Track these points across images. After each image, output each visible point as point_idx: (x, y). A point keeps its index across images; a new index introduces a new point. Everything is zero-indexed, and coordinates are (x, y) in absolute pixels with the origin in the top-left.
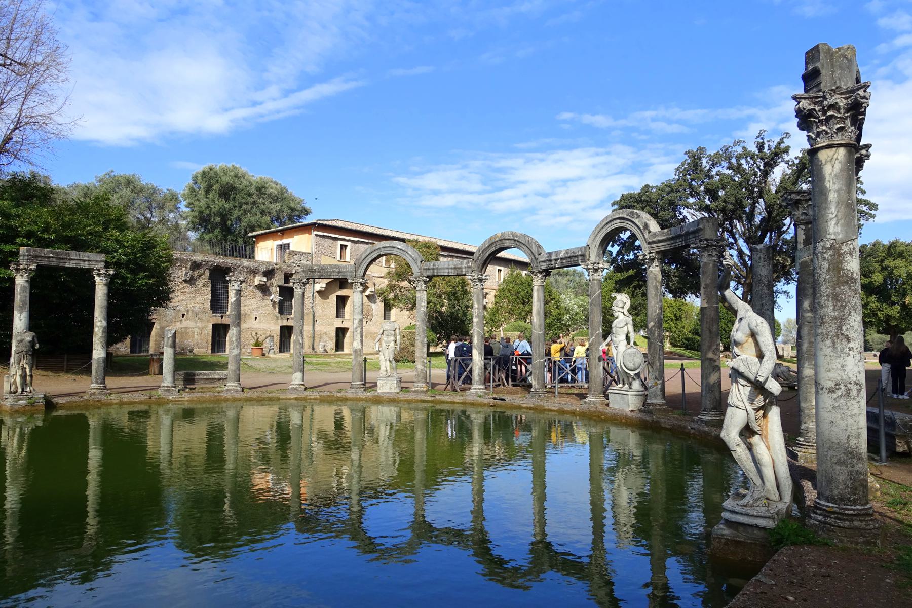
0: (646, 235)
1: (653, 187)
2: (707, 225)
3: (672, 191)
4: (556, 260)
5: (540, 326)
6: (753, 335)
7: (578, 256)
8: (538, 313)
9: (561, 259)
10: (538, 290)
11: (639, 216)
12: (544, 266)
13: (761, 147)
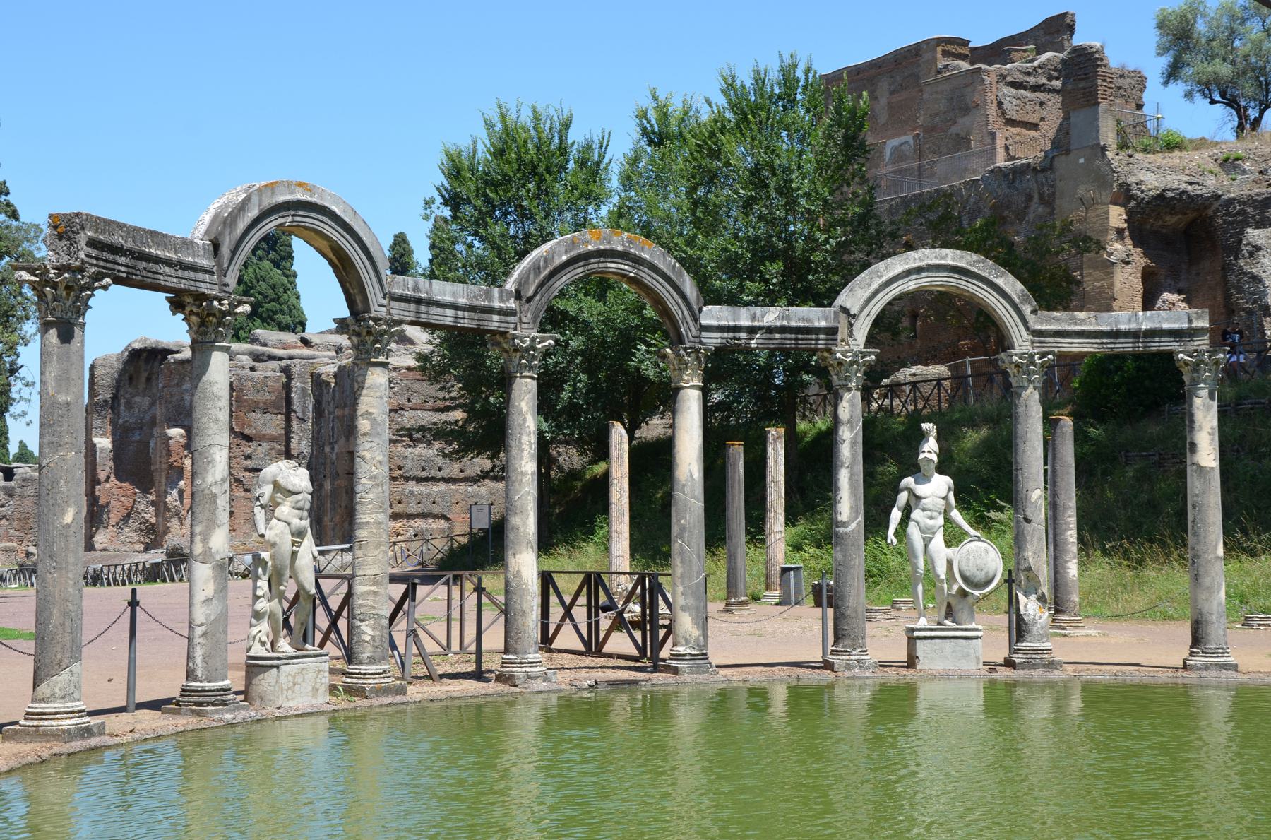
4: (752, 330)
7: (817, 331)
9: (770, 330)
12: (713, 340)
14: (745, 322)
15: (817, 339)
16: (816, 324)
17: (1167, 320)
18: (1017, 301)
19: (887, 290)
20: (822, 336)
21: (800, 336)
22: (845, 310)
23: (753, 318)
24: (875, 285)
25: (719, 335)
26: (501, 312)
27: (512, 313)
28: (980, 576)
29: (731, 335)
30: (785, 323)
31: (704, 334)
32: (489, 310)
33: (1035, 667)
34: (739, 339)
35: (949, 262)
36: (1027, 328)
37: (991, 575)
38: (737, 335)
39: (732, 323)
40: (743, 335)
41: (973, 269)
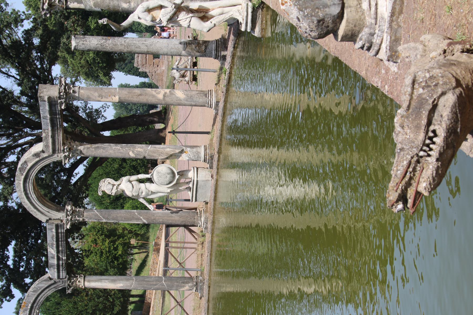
2: (45, 93)
4: (58, 259)
6: (149, 10)
7: (57, 233)
8: (113, 281)
9: (58, 252)
10: (89, 281)
11: (26, 162)
12: (63, 274)
14: (55, 262)
15: (61, 233)
16: (55, 234)
17: (44, 108)
18: (38, 159)
19: (37, 206)
20: (60, 231)
21: (60, 240)
22: (47, 221)
23: (53, 258)
24: (35, 210)
25: (61, 272)
28: (169, 177)
29: (61, 267)
30: (55, 246)
31: (61, 277)
34: (63, 264)
35: (22, 182)
36: (52, 155)
37: (169, 171)
38: (61, 265)
39: (56, 267)
40: (61, 262)
41: (24, 174)
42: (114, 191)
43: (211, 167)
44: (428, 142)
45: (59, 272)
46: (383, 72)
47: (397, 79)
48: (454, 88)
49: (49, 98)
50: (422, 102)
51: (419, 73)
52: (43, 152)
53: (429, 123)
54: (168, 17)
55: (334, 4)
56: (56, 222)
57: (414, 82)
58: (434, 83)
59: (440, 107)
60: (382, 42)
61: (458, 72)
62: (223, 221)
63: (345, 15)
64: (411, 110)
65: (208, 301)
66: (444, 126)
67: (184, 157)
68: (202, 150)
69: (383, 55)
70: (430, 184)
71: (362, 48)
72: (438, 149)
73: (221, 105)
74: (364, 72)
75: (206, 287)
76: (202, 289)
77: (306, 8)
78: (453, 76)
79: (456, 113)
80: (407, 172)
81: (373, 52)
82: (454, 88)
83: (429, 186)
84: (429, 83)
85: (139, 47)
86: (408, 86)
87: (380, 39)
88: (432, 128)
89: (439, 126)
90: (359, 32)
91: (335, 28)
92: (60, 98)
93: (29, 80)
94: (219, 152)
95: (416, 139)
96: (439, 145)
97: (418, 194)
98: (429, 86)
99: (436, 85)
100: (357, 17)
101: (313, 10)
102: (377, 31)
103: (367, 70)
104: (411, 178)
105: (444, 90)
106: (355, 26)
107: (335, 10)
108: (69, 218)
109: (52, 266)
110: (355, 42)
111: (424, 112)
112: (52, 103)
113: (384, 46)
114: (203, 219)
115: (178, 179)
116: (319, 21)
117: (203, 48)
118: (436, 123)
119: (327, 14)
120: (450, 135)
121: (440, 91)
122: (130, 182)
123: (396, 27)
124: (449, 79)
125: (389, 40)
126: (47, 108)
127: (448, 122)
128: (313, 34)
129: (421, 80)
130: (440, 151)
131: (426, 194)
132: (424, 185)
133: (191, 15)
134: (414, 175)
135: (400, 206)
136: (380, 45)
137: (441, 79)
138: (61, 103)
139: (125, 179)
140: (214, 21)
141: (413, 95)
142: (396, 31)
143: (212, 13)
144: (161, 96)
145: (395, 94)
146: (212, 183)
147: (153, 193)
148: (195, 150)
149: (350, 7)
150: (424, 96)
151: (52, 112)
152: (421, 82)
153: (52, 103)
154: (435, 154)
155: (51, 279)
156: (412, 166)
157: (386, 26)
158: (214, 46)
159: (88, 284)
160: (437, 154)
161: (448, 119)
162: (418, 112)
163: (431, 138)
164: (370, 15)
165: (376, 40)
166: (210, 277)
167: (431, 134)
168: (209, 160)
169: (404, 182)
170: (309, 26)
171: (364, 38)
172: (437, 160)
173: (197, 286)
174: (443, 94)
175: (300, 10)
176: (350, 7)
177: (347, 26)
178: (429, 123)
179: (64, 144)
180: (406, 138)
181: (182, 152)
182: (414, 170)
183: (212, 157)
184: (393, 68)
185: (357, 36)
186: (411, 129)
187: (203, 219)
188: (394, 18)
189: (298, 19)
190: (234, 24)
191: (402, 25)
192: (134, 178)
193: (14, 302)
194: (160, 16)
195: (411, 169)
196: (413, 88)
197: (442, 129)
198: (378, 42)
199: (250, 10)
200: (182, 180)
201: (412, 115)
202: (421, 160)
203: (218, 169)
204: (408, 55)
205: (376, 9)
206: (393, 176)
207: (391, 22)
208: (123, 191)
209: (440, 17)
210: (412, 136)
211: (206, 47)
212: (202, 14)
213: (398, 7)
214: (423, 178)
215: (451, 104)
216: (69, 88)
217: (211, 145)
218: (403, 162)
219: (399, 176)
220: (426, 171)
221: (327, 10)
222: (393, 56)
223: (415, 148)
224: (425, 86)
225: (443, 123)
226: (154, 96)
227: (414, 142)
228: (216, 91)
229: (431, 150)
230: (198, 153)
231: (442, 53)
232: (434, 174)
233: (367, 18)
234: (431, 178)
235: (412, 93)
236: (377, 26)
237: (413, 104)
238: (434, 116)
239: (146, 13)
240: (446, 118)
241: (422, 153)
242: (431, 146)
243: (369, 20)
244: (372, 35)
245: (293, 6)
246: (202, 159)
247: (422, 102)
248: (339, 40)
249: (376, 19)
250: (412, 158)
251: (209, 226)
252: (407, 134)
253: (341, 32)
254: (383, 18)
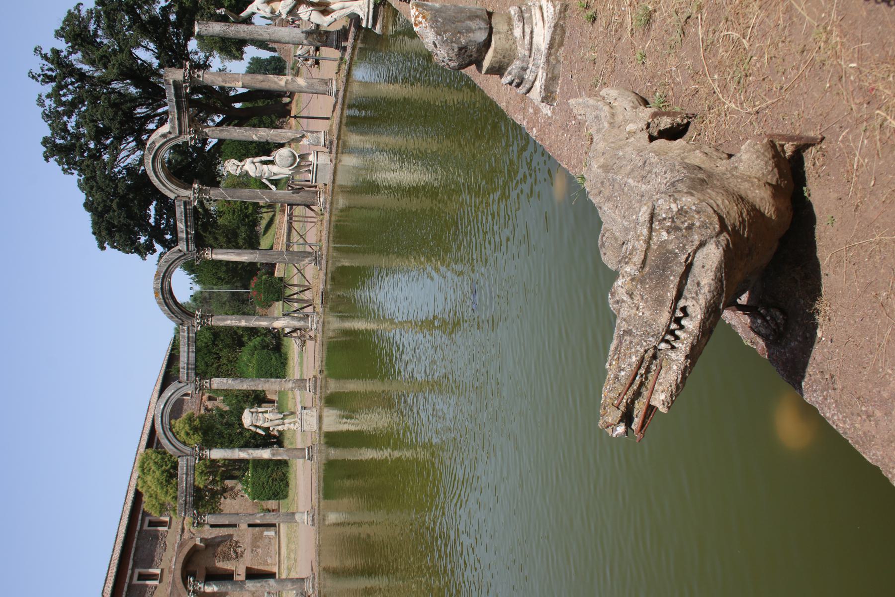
0: (172, 136)
1: (87, 199)
3: (93, 178)
4: (187, 233)
5: (252, 253)
8: (239, 254)
9: (187, 226)
10: (216, 254)
11: (153, 142)
12: (192, 247)
13: (51, 79)
14: (184, 236)
23: (182, 232)
26: (188, 333)
27: (188, 328)
28: (290, 160)
32: (188, 337)
33: (331, 148)
42: (238, 172)
43: (330, 152)
44: (673, 326)
45: (188, 245)
46: (531, 111)
47: (550, 124)
48: (718, 235)
49: (174, 82)
50: (666, 258)
51: (660, 202)
52: (170, 133)
53: (679, 296)
54: (288, 9)
55: (480, 29)
56: (184, 199)
57: (652, 216)
58: (686, 224)
59: (696, 269)
60: (535, 79)
61: (720, 202)
62: (342, 202)
63: (493, 43)
64: (647, 269)
65: (326, 274)
66: (702, 302)
67: (305, 142)
68: (322, 135)
69: (536, 94)
70: (671, 396)
71: (511, 83)
72: (690, 340)
73: (341, 94)
74: (504, 104)
75: (324, 262)
76: (320, 263)
77: (445, 32)
78: (715, 211)
79: (721, 281)
80: (636, 375)
81: (522, 90)
82: (718, 235)
83: (669, 399)
84: (678, 222)
85: (261, 35)
86: (642, 225)
87: (534, 75)
88: (682, 303)
89: (694, 302)
90: (508, 65)
91: (480, 59)
92: (184, 82)
93: (166, 54)
94: (339, 138)
95: (655, 320)
96: (690, 333)
97: (650, 409)
98: (677, 229)
99: (690, 228)
100: (507, 46)
101: (454, 35)
102: (530, 66)
103: (508, 102)
104: (642, 384)
105: (703, 238)
106: (504, 57)
107: (481, 36)
108: (196, 196)
109: (182, 239)
110: (501, 75)
111: (672, 278)
112: (177, 86)
113: (538, 84)
114: (322, 200)
115: (300, 161)
116: (460, 49)
117: (325, 38)
118: (689, 296)
119: (470, 41)
120: (710, 316)
121: (696, 239)
122: (254, 163)
123: (554, 62)
124: (709, 217)
125: (544, 78)
126: (173, 91)
127: (709, 296)
128: (452, 64)
129: (664, 216)
130: (692, 343)
131: (663, 409)
132: (662, 397)
133: (311, 8)
134: (646, 378)
135: (621, 429)
136: (534, 82)
137: (697, 216)
138: (186, 87)
139: (248, 160)
140: (334, 15)
141: (651, 242)
142: (554, 67)
143: (333, 7)
144: (282, 83)
145: (547, 143)
146: (332, 166)
147: (275, 174)
148: (315, 135)
149: (499, 33)
150: (671, 247)
151: (178, 95)
152: (665, 219)
153: (177, 86)
154: (683, 347)
155: (180, 251)
156: (645, 365)
157: (541, 61)
158: (335, 37)
159: (214, 257)
160: (688, 349)
161: (709, 292)
162: (661, 275)
163: (678, 321)
164: (523, 45)
165: (529, 76)
166: (328, 252)
167: (679, 314)
168: (329, 145)
169: (630, 393)
170: (448, 54)
171: (514, 72)
172: (687, 357)
173: (317, 260)
174: (702, 244)
175: (438, 33)
176: (499, 33)
177: (494, 57)
178: (679, 296)
179: (190, 126)
180: (636, 314)
181: (303, 136)
182: (648, 370)
183: (331, 143)
184: (546, 110)
185: (506, 69)
186: (646, 302)
187: (322, 200)
188: (553, 51)
189: (434, 44)
190: (355, 19)
191: (562, 60)
192: (257, 159)
193: (156, 255)
194: (280, 8)
195: (642, 371)
196: (651, 229)
197: (698, 308)
198: (531, 78)
199: (371, 6)
200: (303, 163)
201: (651, 280)
202: (658, 353)
203: (337, 154)
204: (583, 112)
205: (532, 38)
206: (611, 375)
207: (549, 55)
208: (247, 172)
209: (622, 63)
210: (647, 313)
211: (327, 37)
212: (322, 8)
213: (557, 38)
214: (661, 384)
215: (714, 266)
216: (194, 72)
217: (331, 131)
218: (630, 357)
219: (623, 381)
220: (666, 373)
221: (471, 35)
222: (548, 97)
223: (652, 336)
224: (670, 227)
225: (700, 296)
226: (276, 83)
227: (650, 326)
228: (336, 80)
229: (677, 338)
230: (318, 138)
231: (645, 127)
232: (679, 380)
233: (519, 48)
234: (674, 386)
235: (650, 238)
236: (531, 59)
237: (651, 257)
238: (686, 284)
239: (265, 5)
240: (706, 290)
241: (663, 346)
242: (678, 333)
243: (522, 51)
244: (524, 69)
245: (429, 28)
246: (322, 144)
247: (668, 258)
248: (483, 72)
249: (531, 50)
250: (646, 351)
251: (328, 206)
252: (638, 309)
253: (486, 63)
254: (539, 50)
